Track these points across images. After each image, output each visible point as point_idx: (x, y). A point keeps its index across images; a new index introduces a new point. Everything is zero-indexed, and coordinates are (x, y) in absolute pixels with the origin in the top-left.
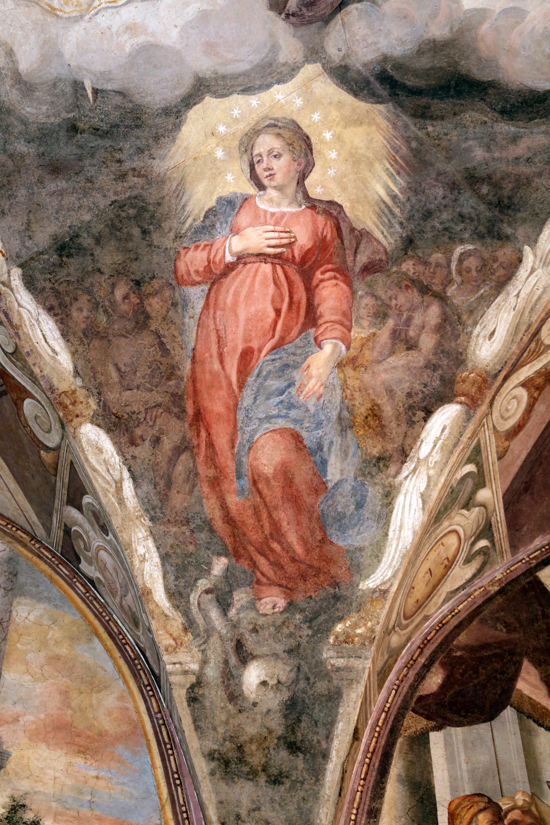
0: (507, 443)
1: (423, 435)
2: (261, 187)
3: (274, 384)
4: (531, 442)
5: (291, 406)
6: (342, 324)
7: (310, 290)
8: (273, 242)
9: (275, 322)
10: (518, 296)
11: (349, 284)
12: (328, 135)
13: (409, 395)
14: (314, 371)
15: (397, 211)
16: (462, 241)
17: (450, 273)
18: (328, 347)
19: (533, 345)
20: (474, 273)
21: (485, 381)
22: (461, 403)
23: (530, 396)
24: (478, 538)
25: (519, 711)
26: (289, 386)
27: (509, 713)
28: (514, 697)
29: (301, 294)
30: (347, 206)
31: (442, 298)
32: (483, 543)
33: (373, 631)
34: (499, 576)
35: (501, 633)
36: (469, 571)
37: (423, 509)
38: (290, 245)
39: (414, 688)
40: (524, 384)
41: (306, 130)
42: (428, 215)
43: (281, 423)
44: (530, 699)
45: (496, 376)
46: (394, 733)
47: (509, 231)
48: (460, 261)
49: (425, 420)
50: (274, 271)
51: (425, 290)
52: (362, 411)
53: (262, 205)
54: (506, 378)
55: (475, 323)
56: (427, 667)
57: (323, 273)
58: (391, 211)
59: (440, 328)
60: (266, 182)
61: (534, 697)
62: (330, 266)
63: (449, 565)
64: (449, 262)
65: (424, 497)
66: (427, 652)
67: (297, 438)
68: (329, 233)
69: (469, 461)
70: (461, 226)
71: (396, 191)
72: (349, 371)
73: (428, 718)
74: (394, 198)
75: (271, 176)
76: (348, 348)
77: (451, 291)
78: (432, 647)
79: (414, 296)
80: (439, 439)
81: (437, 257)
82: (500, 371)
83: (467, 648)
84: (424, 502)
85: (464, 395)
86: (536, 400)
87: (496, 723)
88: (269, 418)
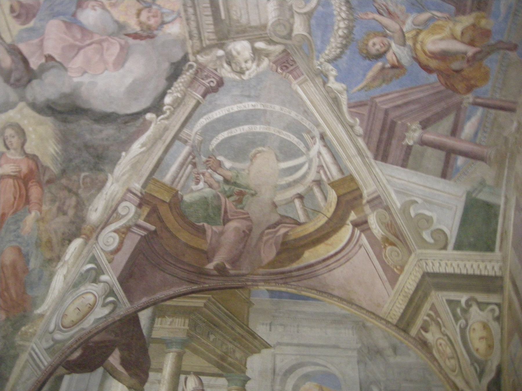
0: (112, 256)
1: (67, 251)
2: (8, 148)
3: (12, 227)
4: (128, 256)
5: (18, 237)
6: (39, 204)
7: (27, 190)
8: (14, 170)
9: (14, 203)
10: (106, 194)
11: (41, 187)
12: (31, 129)
13: (63, 234)
14: (28, 223)
15: (59, 159)
16: (84, 171)
17: (79, 184)
18: (33, 214)
19: (115, 215)
20: (89, 184)
21: (93, 229)
22: (83, 238)
23: (120, 237)
24: (107, 296)
25: (105, 369)
26: (18, 228)
27: (101, 370)
28: (105, 364)
29: (24, 191)
30: (40, 157)
31: (77, 194)
32: (111, 299)
33: (36, 331)
34: (122, 313)
35: (112, 337)
36: (106, 311)
37: (64, 282)
38: (19, 172)
39: (67, 357)
40: (116, 231)
41: (23, 127)
42: (71, 160)
43: (14, 244)
44: (112, 364)
45: (97, 227)
46: (51, 374)
47: (102, 167)
48: (84, 179)
49: (69, 244)
50: (14, 182)
51: (70, 191)
52: (44, 239)
53: (9, 156)
54: (103, 228)
55: (90, 205)
56: (76, 349)
57: (32, 183)
58: (56, 159)
59: (76, 207)
60: (10, 146)
61: (114, 364)
62: (34, 180)
63: (92, 308)
64: (79, 179)
65: (65, 277)
66: (78, 343)
67: (20, 250)
68: (34, 167)
69: (90, 262)
70: (83, 165)
71: (58, 151)
72: (41, 223)
73: (67, 369)
74: (57, 153)
75: (12, 144)
76: (41, 213)
77: (80, 191)
78: (82, 341)
79: (66, 193)
80: (73, 252)
81: (75, 177)
82: (99, 225)
83: (96, 343)
84: (65, 279)
85: (85, 234)
86: (124, 238)
87: (94, 373)
88: (10, 241)
